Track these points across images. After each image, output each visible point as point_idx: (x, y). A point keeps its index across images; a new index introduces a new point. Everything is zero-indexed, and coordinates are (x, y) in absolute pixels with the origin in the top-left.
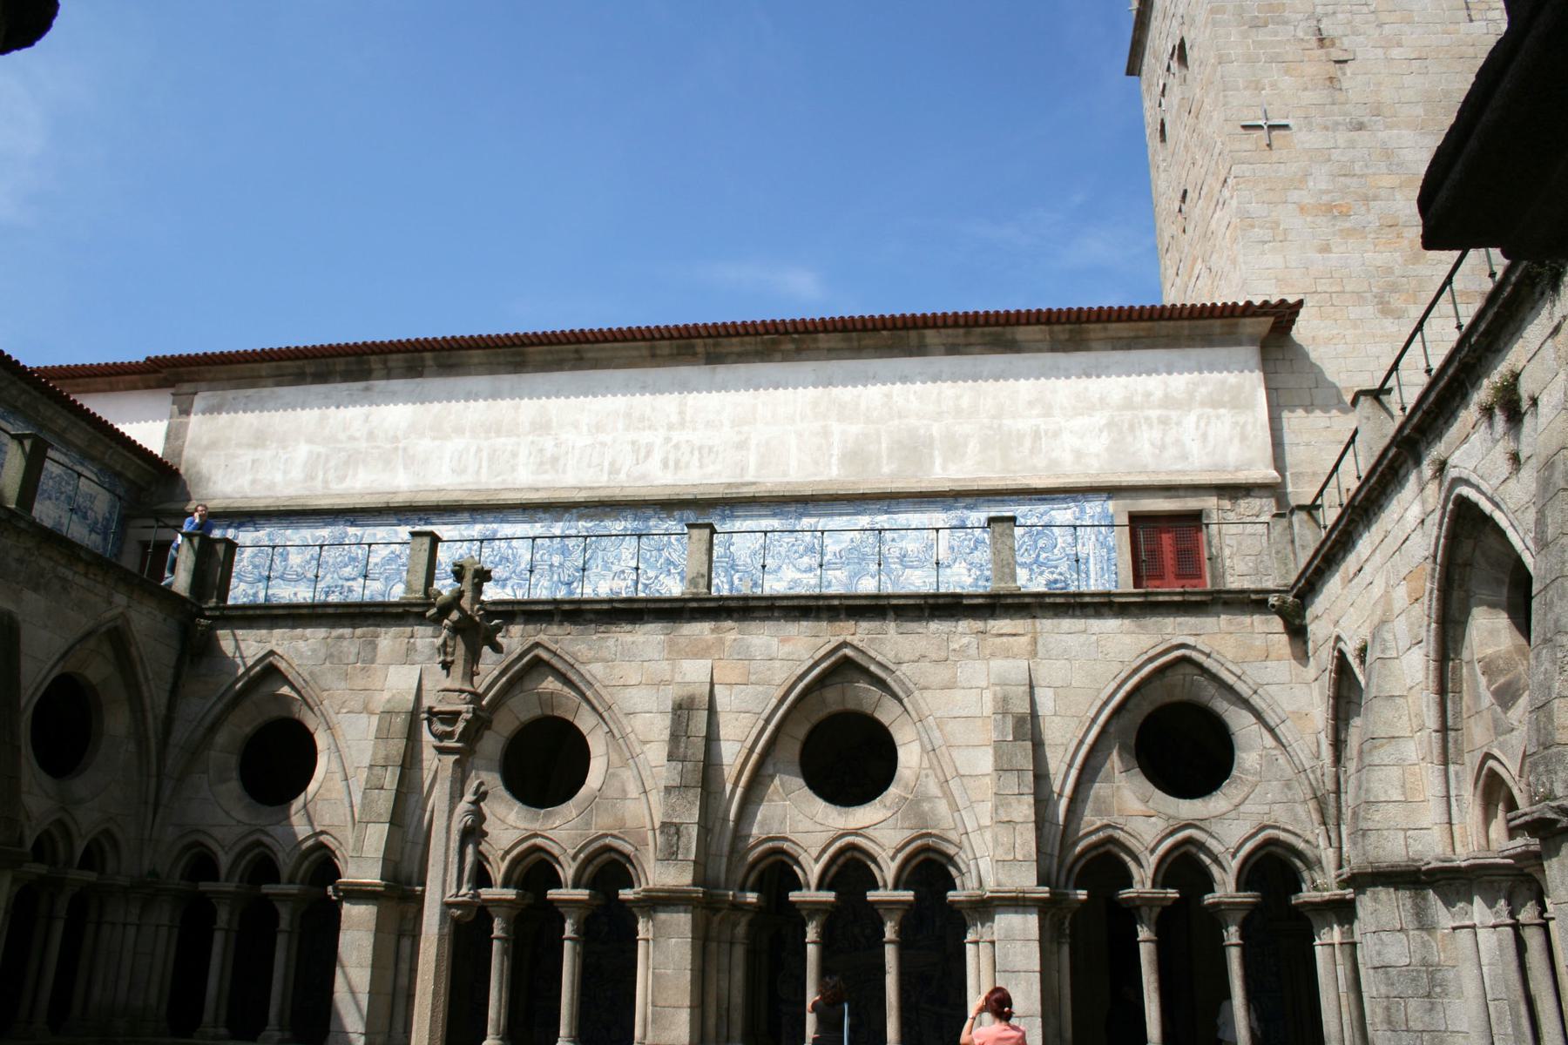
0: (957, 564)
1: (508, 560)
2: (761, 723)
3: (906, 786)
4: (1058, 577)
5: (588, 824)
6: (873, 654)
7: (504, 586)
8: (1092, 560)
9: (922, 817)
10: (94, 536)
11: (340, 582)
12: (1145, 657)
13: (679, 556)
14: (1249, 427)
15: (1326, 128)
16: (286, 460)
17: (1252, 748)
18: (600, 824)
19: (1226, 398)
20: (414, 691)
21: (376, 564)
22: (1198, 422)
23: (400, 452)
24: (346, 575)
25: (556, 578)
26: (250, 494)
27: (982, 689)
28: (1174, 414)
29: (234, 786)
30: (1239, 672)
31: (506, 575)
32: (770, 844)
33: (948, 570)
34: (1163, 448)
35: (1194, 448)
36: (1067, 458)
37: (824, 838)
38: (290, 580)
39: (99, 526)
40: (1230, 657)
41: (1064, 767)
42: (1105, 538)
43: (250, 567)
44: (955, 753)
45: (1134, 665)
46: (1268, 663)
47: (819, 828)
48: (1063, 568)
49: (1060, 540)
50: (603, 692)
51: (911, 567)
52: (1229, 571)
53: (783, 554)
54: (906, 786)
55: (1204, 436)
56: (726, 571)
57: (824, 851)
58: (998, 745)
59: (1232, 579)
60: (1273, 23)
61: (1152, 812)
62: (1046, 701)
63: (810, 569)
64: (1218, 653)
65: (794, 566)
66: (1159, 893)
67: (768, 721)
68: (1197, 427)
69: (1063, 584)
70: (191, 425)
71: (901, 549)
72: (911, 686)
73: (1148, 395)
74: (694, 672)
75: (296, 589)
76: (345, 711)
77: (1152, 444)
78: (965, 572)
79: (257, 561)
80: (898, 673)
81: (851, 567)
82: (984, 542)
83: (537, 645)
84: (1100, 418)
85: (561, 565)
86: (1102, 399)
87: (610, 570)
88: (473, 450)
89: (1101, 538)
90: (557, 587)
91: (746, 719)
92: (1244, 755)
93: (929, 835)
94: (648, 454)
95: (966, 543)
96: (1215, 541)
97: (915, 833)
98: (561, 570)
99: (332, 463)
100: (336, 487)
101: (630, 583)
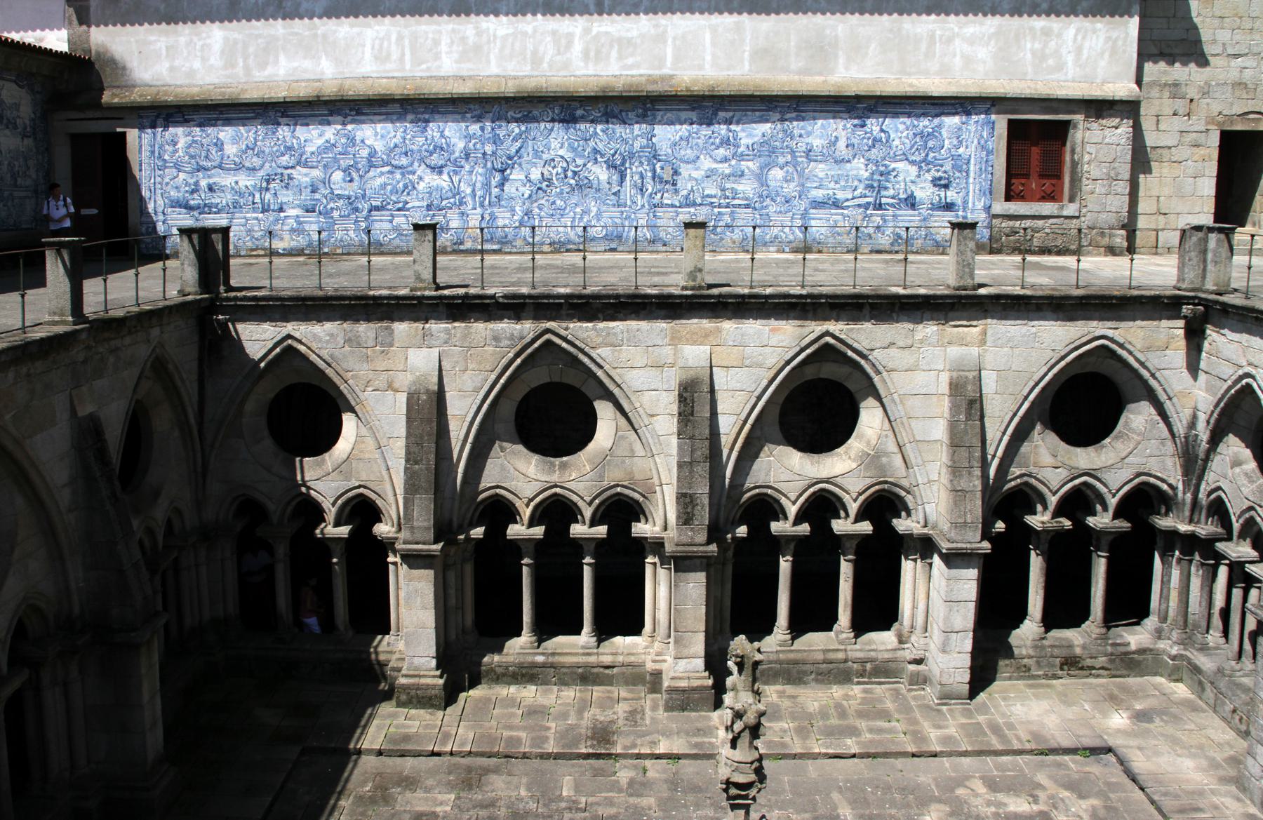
0: (856, 160)
1: (442, 149)
2: (753, 400)
3: (868, 443)
4: (943, 175)
5: (601, 477)
6: (850, 341)
7: (440, 173)
8: (972, 161)
9: (882, 469)
10: (26, 141)
11: (279, 171)
12: (1072, 346)
13: (605, 146)
14: (1120, 43)
16: (203, 46)
17: (1139, 413)
18: (614, 476)
20: (437, 373)
21: (313, 153)
23: (320, 39)
24: (284, 164)
25: (489, 165)
26: (169, 80)
27: (940, 371)
29: (268, 443)
30: (1143, 359)
31: (441, 162)
32: (757, 491)
33: (848, 164)
34: (1043, 58)
37: (801, 485)
38: (229, 170)
39: (28, 129)
40: (1139, 346)
41: (999, 434)
42: (986, 142)
43: (187, 158)
44: (914, 423)
45: (1063, 353)
46: (1168, 352)
47: (798, 478)
48: (948, 167)
49: (947, 142)
50: (612, 373)
51: (816, 161)
52: (1086, 175)
53: (701, 145)
54: (868, 443)
56: (649, 161)
57: (801, 495)
58: (953, 426)
59: (1087, 182)
61: (1060, 464)
62: (989, 383)
63: (725, 160)
64: (1130, 343)
65: (711, 157)
66: (1054, 524)
67: (759, 398)
69: (946, 181)
70: (92, 9)
71: (807, 144)
72: (880, 368)
74: (695, 355)
75: (236, 178)
76: (370, 389)
78: (863, 166)
79: (192, 151)
80: (870, 357)
81: (762, 159)
82: (881, 140)
83: (548, 331)
85: (494, 153)
87: (540, 158)
88: (394, 38)
89: (982, 142)
90: (491, 174)
91: (741, 397)
92: (1132, 416)
93: (886, 482)
94: (570, 44)
95: (865, 141)
96: (1078, 150)
97: (874, 481)
98: (493, 158)
99: (251, 50)
100: (258, 74)
101: (560, 170)
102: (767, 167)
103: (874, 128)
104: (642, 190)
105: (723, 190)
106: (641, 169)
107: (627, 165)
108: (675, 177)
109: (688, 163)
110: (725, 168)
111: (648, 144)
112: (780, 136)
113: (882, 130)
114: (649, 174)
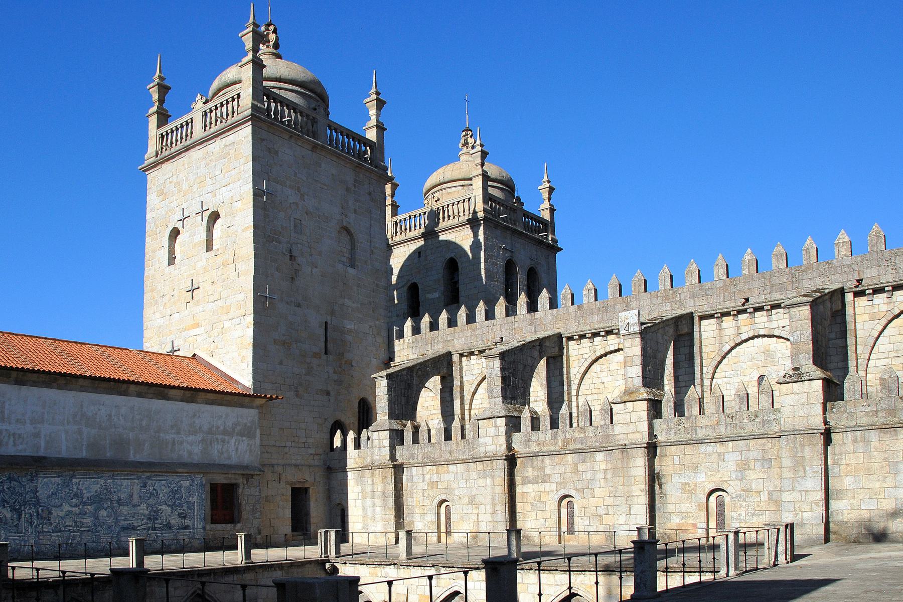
14: (253, 447)
15: (287, 303)
19: (246, 433)
22: (235, 442)
28: (227, 438)
34: (222, 453)
35: (233, 454)
36: (185, 454)
51: (123, 505)
53: (63, 497)
55: (237, 449)
60: (276, 242)
63: (76, 506)
65: (69, 504)
68: (235, 445)
73: (218, 427)
77: (218, 451)
82: (154, 494)
84: (199, 437)
86: (200, 428)
102: (98, 509)
103: (150, 488)
104: (31, 523)
105: (76, 522)
106: (30, 511)
107: (23, 508)
108: (49, 516)
109: (58, 507)
110: (76, 510)
111: (34, 497)
112: (105, 492)
113: (154, 489)
114: (35, 514)
